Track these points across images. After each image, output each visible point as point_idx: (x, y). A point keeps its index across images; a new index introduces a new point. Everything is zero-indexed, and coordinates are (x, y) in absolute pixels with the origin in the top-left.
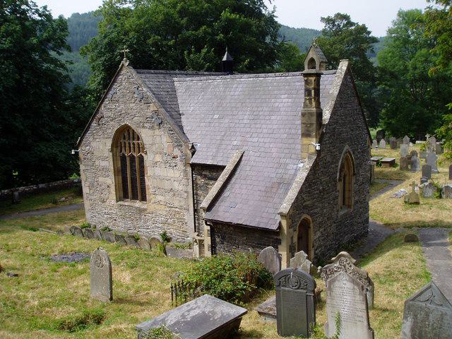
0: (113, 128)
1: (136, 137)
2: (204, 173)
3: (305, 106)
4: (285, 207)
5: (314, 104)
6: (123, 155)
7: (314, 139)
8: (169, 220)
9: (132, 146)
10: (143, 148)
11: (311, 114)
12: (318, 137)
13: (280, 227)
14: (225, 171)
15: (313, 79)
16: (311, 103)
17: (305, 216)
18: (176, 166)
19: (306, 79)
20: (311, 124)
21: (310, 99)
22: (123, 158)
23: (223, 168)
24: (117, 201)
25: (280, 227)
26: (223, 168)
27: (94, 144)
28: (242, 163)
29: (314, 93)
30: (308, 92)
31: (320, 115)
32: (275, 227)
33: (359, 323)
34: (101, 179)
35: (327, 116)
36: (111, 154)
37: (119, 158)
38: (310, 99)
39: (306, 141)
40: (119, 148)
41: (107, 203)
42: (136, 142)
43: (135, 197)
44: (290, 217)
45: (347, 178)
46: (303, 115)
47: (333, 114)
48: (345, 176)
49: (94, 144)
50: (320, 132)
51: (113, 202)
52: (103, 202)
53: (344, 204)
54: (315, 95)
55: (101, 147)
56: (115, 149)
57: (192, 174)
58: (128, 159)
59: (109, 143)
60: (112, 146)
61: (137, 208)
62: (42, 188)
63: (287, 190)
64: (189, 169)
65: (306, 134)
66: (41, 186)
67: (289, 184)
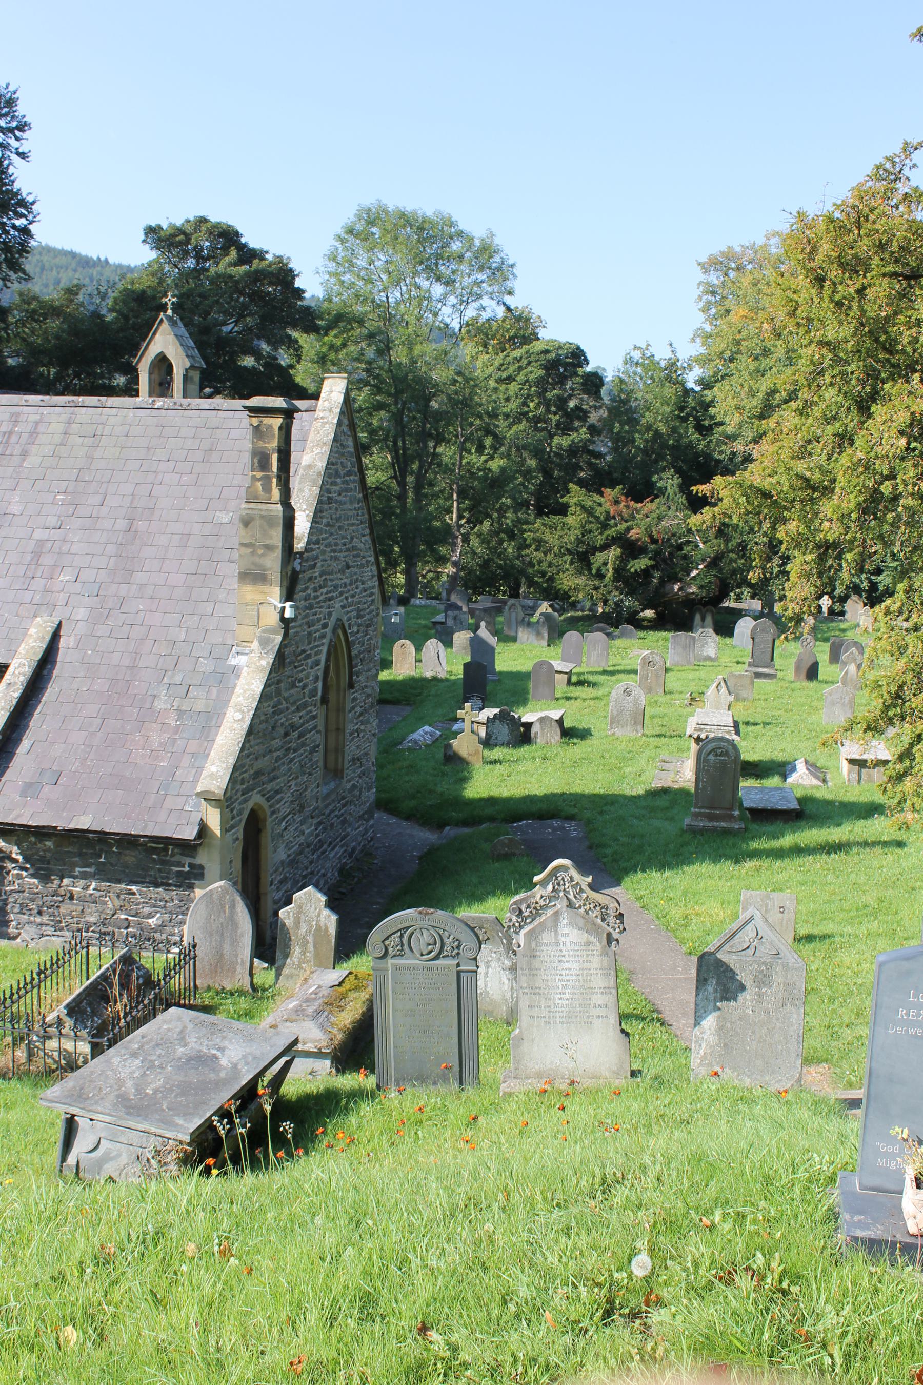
3: (251, 498)
4: (216, 771)
5: (276, 494)
11: (268, 520)
12: (285, 584)
13: (203, 830)
15: (276, 422)
16: (267, 489)
17: (256, 799)
19: (255, 422)
20: (269, 548)
25: (203, 830)
28: (61, 656)
30: (262, 462)
32: (189, 833)
33: (597, 1023)
38: (267, 480)
39: (250, 592)
44: (226, 803)
50: (290, 568)
54: (279, 469)
65: (252, 576)
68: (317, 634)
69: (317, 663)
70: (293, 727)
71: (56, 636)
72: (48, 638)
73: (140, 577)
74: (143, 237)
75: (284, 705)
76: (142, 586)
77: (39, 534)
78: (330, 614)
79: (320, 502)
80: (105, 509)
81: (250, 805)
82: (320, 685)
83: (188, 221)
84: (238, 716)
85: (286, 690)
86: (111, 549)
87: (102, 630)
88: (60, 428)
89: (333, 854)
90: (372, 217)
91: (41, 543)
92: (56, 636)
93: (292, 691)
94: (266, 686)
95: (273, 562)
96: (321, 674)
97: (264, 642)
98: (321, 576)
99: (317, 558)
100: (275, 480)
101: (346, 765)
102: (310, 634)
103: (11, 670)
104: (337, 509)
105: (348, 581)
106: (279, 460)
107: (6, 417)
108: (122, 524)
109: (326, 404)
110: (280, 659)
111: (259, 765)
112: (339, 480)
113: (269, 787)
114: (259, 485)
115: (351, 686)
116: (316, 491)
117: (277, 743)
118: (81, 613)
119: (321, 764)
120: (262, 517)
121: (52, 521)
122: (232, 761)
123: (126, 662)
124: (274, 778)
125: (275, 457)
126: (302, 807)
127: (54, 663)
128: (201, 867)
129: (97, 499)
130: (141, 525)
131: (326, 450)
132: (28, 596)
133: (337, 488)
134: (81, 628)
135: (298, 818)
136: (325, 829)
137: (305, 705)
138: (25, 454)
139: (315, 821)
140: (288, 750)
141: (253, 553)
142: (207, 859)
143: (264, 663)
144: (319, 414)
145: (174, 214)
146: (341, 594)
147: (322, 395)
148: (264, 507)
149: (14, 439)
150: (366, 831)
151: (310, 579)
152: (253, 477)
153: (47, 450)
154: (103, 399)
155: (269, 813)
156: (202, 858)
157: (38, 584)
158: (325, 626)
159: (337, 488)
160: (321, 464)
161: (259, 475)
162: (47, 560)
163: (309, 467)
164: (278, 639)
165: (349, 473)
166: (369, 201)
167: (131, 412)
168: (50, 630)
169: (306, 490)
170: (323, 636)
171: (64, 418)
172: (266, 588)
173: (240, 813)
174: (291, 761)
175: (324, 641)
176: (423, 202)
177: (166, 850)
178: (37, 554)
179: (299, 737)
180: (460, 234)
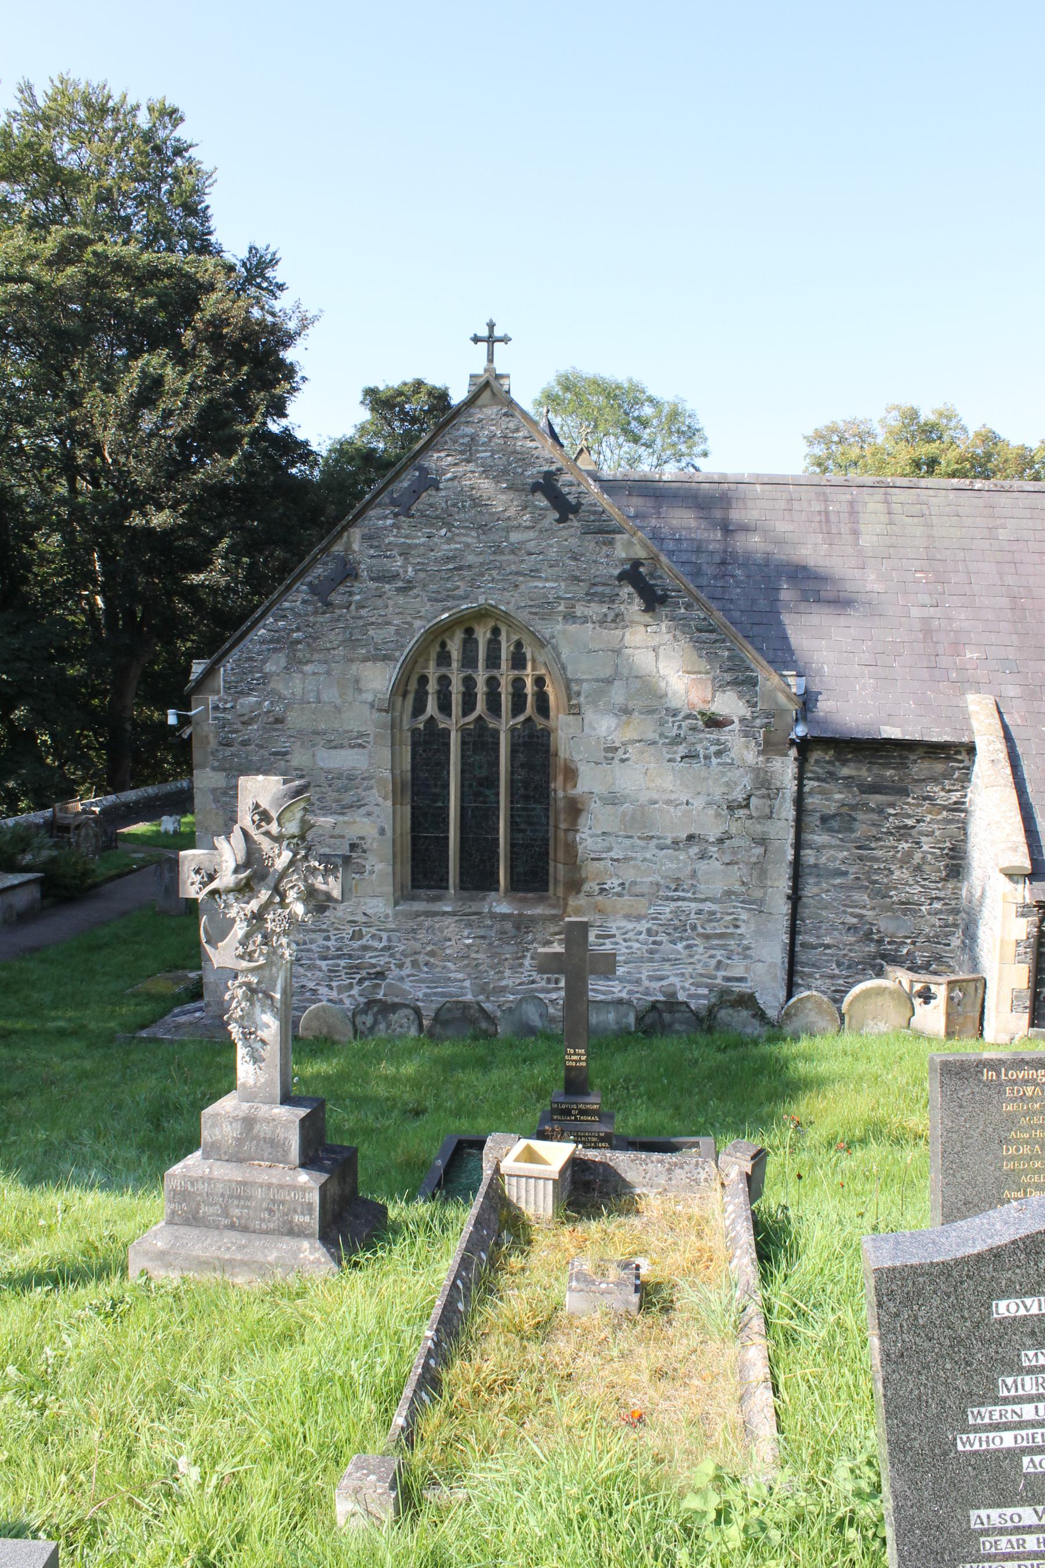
0: (418, 614)
2: (845, 771)
8: (667, 946)
9: (481, 689)
18: (719, 754)
49: (294, 686)
55: (331, 695)
61: (504, 917)
74: (361, 398)
83: (405, 384)
90: (568, 384)
145: (390, 378)
166: (564, 368)
176: (616, 371)
180: (650, 400)
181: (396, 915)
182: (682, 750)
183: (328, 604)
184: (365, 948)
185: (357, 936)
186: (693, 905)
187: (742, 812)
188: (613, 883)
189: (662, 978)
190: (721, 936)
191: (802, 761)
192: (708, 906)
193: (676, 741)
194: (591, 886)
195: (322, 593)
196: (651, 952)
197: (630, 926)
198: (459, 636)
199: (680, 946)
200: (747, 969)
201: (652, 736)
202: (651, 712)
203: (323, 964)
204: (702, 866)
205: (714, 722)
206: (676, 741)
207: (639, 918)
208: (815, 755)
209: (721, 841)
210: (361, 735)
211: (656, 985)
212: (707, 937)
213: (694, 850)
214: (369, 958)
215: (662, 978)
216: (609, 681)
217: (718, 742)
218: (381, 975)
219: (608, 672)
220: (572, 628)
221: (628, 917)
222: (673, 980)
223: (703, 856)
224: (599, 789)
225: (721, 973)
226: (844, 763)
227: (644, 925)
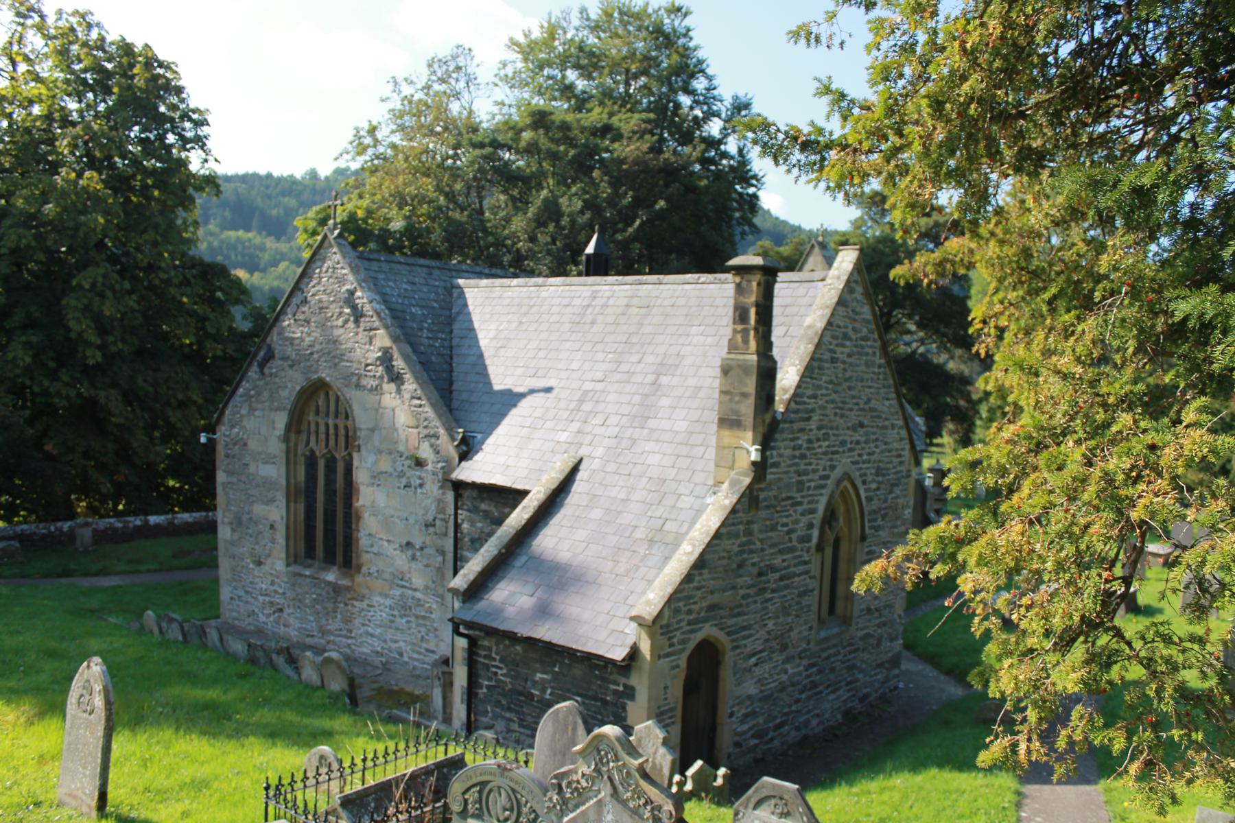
0: (292, 383)
1: (341, 409)
2: (483, 506)
3: (732, 347)
4: (651, 600)
5: (753, 344)
6: (312, 451)
7: (749, 435)
8: (398, 620)
9: (332, 431)
10: (355, 438)
11: (745, 369)
12: (761, 430)
14: (525, 502)
16: (746, 341)
17: (708, 631)
18: (421, 486)
19: (738, 279)
20: (744, 395)
21: (745, 333)
22: (311, 462)
23: (524, 493)
24: (288, 565)
25: (634, 653)
26: (524, 493)
27: (250, 424)
28: (578, 487)
29: (759, 318)
30: (741, 315)
31: (767, 373)
32: (618, 654)
34: (259, 509)
35: (788, 378)
36: (283, 446)
37: (301, 460)
38: (745, 333)
39: (728, 436)
40: (304, 437)
41: (265, 568)
42: (341, 423)
43: (330, 560)
44: (659, 626)
45: (844, 548)
46: (726, 371)
47: (810, 372)
48: (837, 542)
49: (250, 424)
50: (768, 418)
51: (280, 566)
52: (259, 563)
53: (832, 610)
54: (757, 322)
56: (293, 436)
57: (456, 508)
58: (321, 464)
59: (281, 420)
60: (288, 428)
61: (329, 583)
62: (157, 526)
63: (667, 559)
64: (450, 496)
66: (153, 519)
67: (676, 545)
68: (812, 484)
69: (812, 511)
70: (773, 569)
71: (575, 469)
72: (567, 470)
73: (652, 423)
75: (758, 545)
76: (652, 430)
77: (588, 386)
78: (833, 468)
79: (812, 359)
80: (641, 365)
81: (700, 636)
82: (815, 533)
84: (689, 548)
85: (761, 531)
86: (637, 399)
87: (611, 467)
88: (624, 301)
89: (831, 697)
91: (586, 392)
92: (575, 469)
93: (770, 534)
94: (723, 524)
95: (747, 408)
96: (817, 522)
97: (733, 484)
98: (819, 428)
99: (813, 411)
100: (752, 333)
101: (856, 613)
102: (800, 483)
103: (530, 495)
104: (845, 370)
105: (863, 439)
106: (757, 313)
107: (588, 294)
108: (650, 379)
109: (836, 273)
110: (750, 500)
111: (716, 598)
112: (848, 343)
113: (731, 622)
114: (739, 337)
115: (863, 538)
116: (811, 348)
117: (747, 580)
118: (600, 452)
119: (815, 608)
120: (739, 366)
121: (599, 375)
122: (670, 590)
123: (622, 496)
124: (739, 614)
125: (753, 311)
126: (784, 647)
127: (568, 492)
128: (633, 689)
129: (636, 358)
130: (664, 380)
131: (828, 312)
132: (564, 437)
133: (846, 350)
134: (596, 464)
135: (778, 657)
136: (820, 672)
137: (792, 550)
138: (593, 323)
139: (805, 662)
140: (764, 590)
141: (731, 400)
142: (640, 682)
143: (727, 502)
144: (829, 281)
146: (851, 450)
147: (835, 265)
148: (741, 357)
149: (590, 311)
150: (887, 679)
151: (802, 430)
152: (735, 331)
153: (610, 319)
154: (661, 277)
155: (728, 646)
156: (634, 681)
157: (576, 426)
158: (826, 477)
159: (846, 350)
160: (820, 325)
161: (739, 327)
162: (587, 407)
163: (810, 327)
164: (747, 481)
165: (865, 339)
167: (680, 287)
168: (571, 465)
169: (802, 347)
170: (823, 487)
171: (629, 294)
172: (741, 434)
173: (684, 642)
174: (767, 601)
175: (823, 491)
177: (605, 667)
178: (581, 401)
179: (781, 579)
181: (288, 573)
182: (404, 481)
183: (263, 374)
184: (275, 592)
185: (273, 583)
186: (410, 592)
187: (431, 529)
188: (373, 569)
189: (396, 642)
190: (424, 618)
191: (458, 497)
192: (418, 595)
193: (402, 474)
194: (364, 569)
195: (262, 366)
196: (392, 622)
197: (382, 601)
198: (322, 396)
199: (404, 620)
200: (437, 646)
201: (390, 470)
202: (390, 453)
203: (261, 598)
204: (413, 565)
205: (420, 463)
206: (402, 474)
207: (386, 596)
208: (467, 493)
209: (422, 549)
210: (275, 457)
211: (394, 646)
212: (417, 617)
213: (409, 553)
214: (279, 600)
215: (396, 642)
216: (372, 430)
217: (420, 478)
218: (281, 610)
219: (371, 425)
220: (359, 393)
221: (381, 594)
222: (402, 644)
223: (414, 558)
224: (368, 504)
225: (424, 645)
226: (482, 500)
227: (388, 602)
